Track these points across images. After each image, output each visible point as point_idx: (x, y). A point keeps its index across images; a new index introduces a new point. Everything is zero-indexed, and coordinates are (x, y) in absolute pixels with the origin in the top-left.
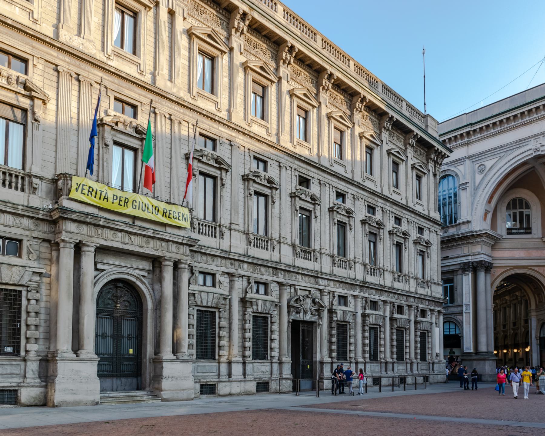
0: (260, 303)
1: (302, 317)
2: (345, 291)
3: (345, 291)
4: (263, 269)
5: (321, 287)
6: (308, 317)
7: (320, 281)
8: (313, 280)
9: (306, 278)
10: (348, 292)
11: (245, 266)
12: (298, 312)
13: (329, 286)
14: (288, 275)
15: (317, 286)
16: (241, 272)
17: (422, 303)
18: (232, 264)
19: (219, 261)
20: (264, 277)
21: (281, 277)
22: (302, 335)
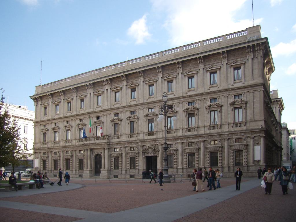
0: (130, 153)
1: (149, 155)
2: (171, 142)
3: (171, 142)
4: (132, 143)
5: (157, 144)
6: (152, 155)
7: (158, 142)
8: (153, 142)
9: (150, 142)
10: (173, 142)
11: (127, 144)
12: (148, 154)
13: (162, 142)
14: (142, 143)
15: (156, 144)
16: (126, 146)
17: (236, 135)
18: (123, 144)
19: (119, 145)
20: (134, 145)
21: (140, 144)
22: (151, 161)
